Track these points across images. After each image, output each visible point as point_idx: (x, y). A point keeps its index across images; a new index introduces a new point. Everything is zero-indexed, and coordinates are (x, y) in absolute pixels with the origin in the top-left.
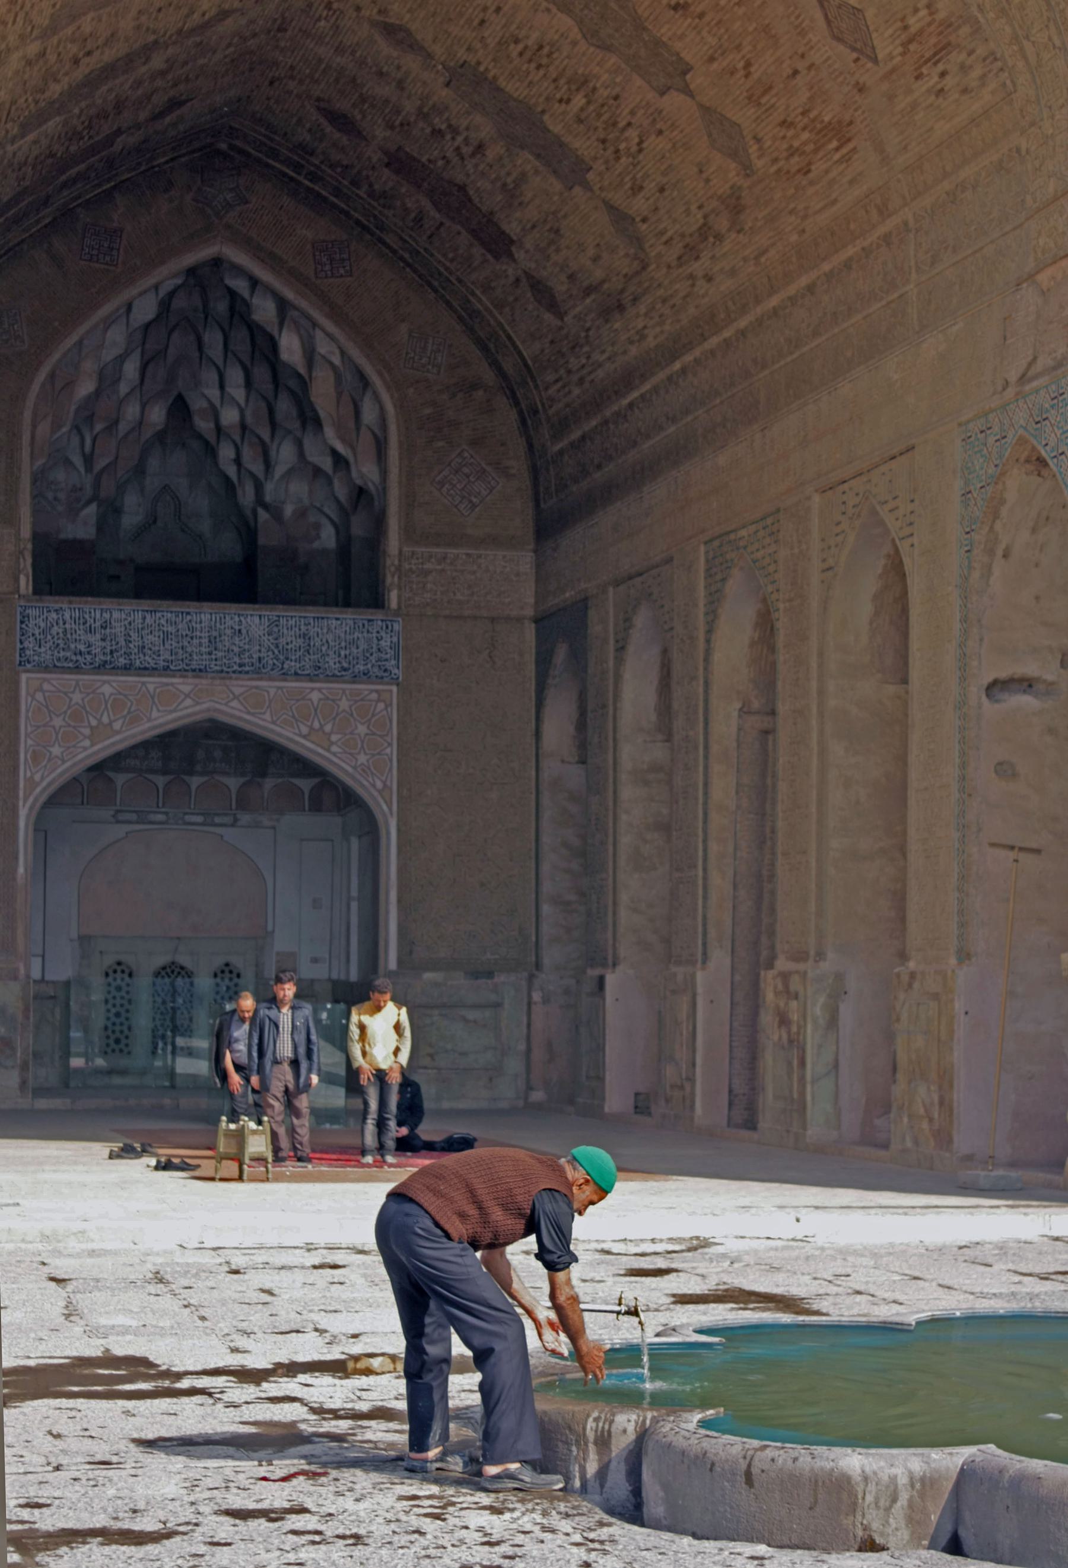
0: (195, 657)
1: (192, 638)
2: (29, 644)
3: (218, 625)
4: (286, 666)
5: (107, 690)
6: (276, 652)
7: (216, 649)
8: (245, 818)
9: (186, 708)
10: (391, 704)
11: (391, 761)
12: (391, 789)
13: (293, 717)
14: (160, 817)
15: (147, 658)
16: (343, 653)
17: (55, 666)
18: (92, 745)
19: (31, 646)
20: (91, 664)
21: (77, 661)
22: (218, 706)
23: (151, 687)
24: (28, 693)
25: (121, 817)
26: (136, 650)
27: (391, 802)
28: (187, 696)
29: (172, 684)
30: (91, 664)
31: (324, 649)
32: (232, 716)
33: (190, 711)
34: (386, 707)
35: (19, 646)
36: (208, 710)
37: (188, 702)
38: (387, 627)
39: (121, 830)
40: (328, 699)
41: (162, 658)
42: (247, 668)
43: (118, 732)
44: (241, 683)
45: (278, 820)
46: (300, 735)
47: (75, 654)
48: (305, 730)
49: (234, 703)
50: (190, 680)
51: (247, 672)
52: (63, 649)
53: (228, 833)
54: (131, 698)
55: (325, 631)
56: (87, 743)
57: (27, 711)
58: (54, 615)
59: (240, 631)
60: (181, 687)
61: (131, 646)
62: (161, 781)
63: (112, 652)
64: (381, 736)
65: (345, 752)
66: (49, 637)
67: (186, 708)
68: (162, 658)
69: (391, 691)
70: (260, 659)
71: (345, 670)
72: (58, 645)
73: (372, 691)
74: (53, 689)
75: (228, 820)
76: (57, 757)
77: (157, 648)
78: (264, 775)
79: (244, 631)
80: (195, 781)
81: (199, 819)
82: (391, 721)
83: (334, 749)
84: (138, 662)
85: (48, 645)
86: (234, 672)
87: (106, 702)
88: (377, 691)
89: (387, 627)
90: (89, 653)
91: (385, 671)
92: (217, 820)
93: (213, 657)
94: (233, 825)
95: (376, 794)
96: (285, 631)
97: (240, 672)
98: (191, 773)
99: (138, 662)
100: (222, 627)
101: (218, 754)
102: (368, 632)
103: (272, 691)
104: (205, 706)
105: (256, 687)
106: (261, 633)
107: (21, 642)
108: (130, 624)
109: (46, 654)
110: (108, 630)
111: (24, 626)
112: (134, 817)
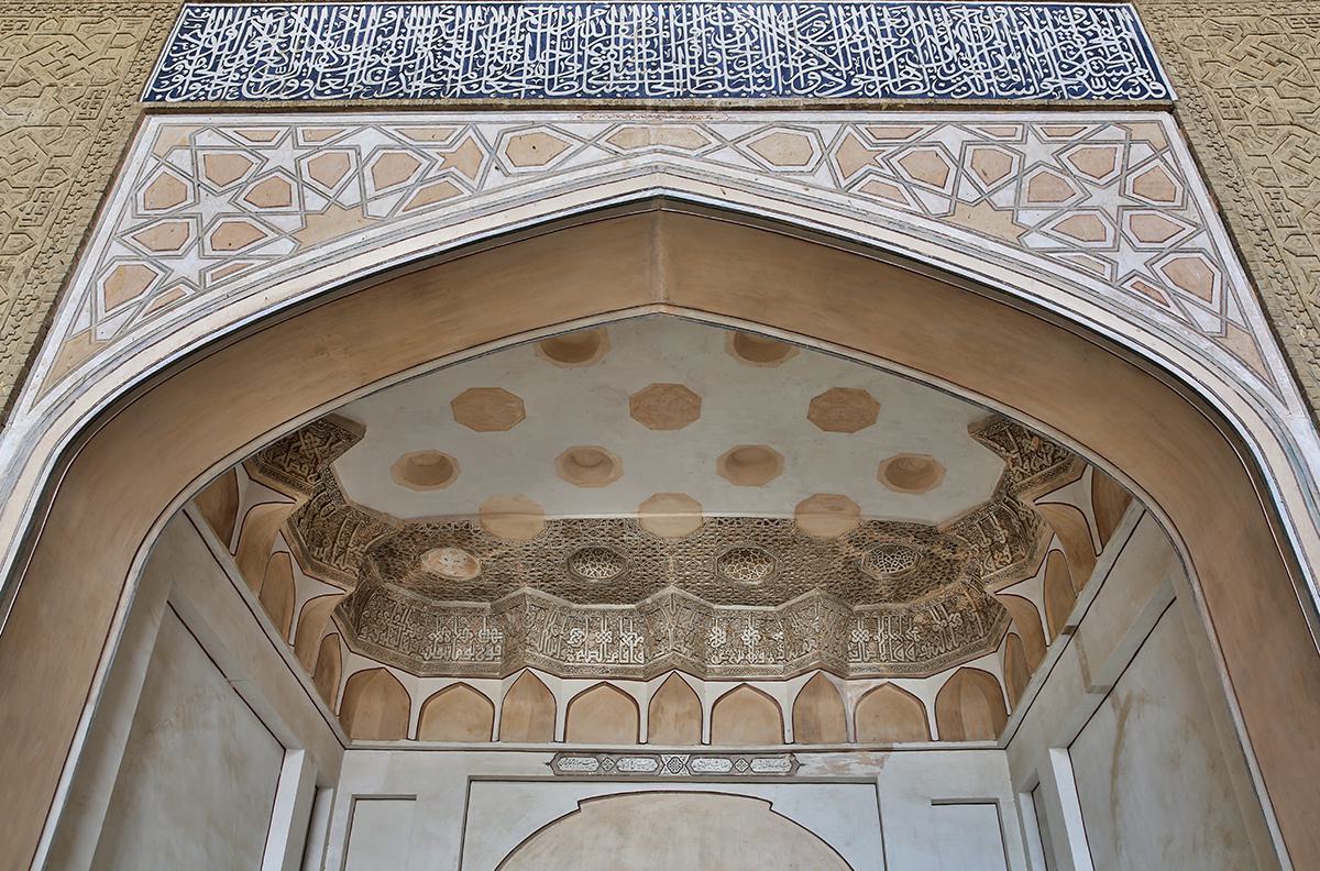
0: (613, 72)
1: (606, 43)
2: (188, 66)
3: (673, 22)
4: (858, 81)
5: (368, 140)
6: (828, 60)
7: (666, 60)
8: (813, 764)
9: (587, 166)
10: (1168, 145)
11: (1219, 263)
12: (1248, 329)
13: (898, 178)
14: (646, 765)
15: (485, 78)
16: (1003, 59)
17: (241, 97)
18: (296, 253)
19: (192, 68)
20: (334, 92)
21: (301, 89)
22: (676, 160)
23: (490, 133)
24: (152, 153)
25: (567, 765)
26: (460, 67)
27: (1266, 366)
28: (593, 142)
29: (549, 125)
30: (334, 92)
31: (952, 53)
32: (722, 183)
33: (594, 171)
34: (1157, 153)
35: (161, 66)
36: (653, 169)
37: (593, 154)
38: (1102, 17)
39: (566, 796)
40: (987, 141)
41: (525, 77)
42: (753, 88)
43: (380, 221)
44: (738, 116)
45: (880, 763)
46: (926, 216)
47: (300, 78)
48: (937, 205)
49: (726, 155)
50: (599, 115)
51: (757, 95)
52: (272, 71)
53: (783, 797)
54: (431, 152)
55: (947, 24)
56: (285, 246)
57: (137, 186)
58: (269, 20)
59: (728, 29)
60: (570, 128)
61: (451, 61)
62: (642, 691)
63: (395, 72)
64: (1166, 210)
65: (1073, 249)
66: (243, 52)
67: (587, 166)
68: (525, 77)
69: (1159, 123)
70: (785, 71)
71: (1019, 87)
72: (261, 63)
73: (1105, 125)
74: (225, 143)
75: (780, 765)
76: (185, 281)
77: (513, 62)
78: (841, 673)
79: (739, 30)
80: (710, 691)
81: (722, 766)
82: (1183, 181)
83: (1035, 241)
84: (460, 86)
85: (235, 66)
86: (721, 94)
87: (361, 165)
88: (1118, 124)
89: (1102, 17)
90: (334, 75)
91: (1126, 86)
92: (758, 766)
93: (662, 71)
94: (790, 779)
95: (1205, 345)
96: (845, 27)
97: (738, 95)
98: (702, 675)
99: (460, 86)
100: (685, 24)
101: (750, 634)
102: (1056, 25)
103: (829, 133)
104: (640, 161)
105: (784, 125)
106: (785, 31)
107: (169, 61)
108: (452, 26)
109: (224, 81)
110: (394, 38)
111: (186, 37)
112: (591, 764)
